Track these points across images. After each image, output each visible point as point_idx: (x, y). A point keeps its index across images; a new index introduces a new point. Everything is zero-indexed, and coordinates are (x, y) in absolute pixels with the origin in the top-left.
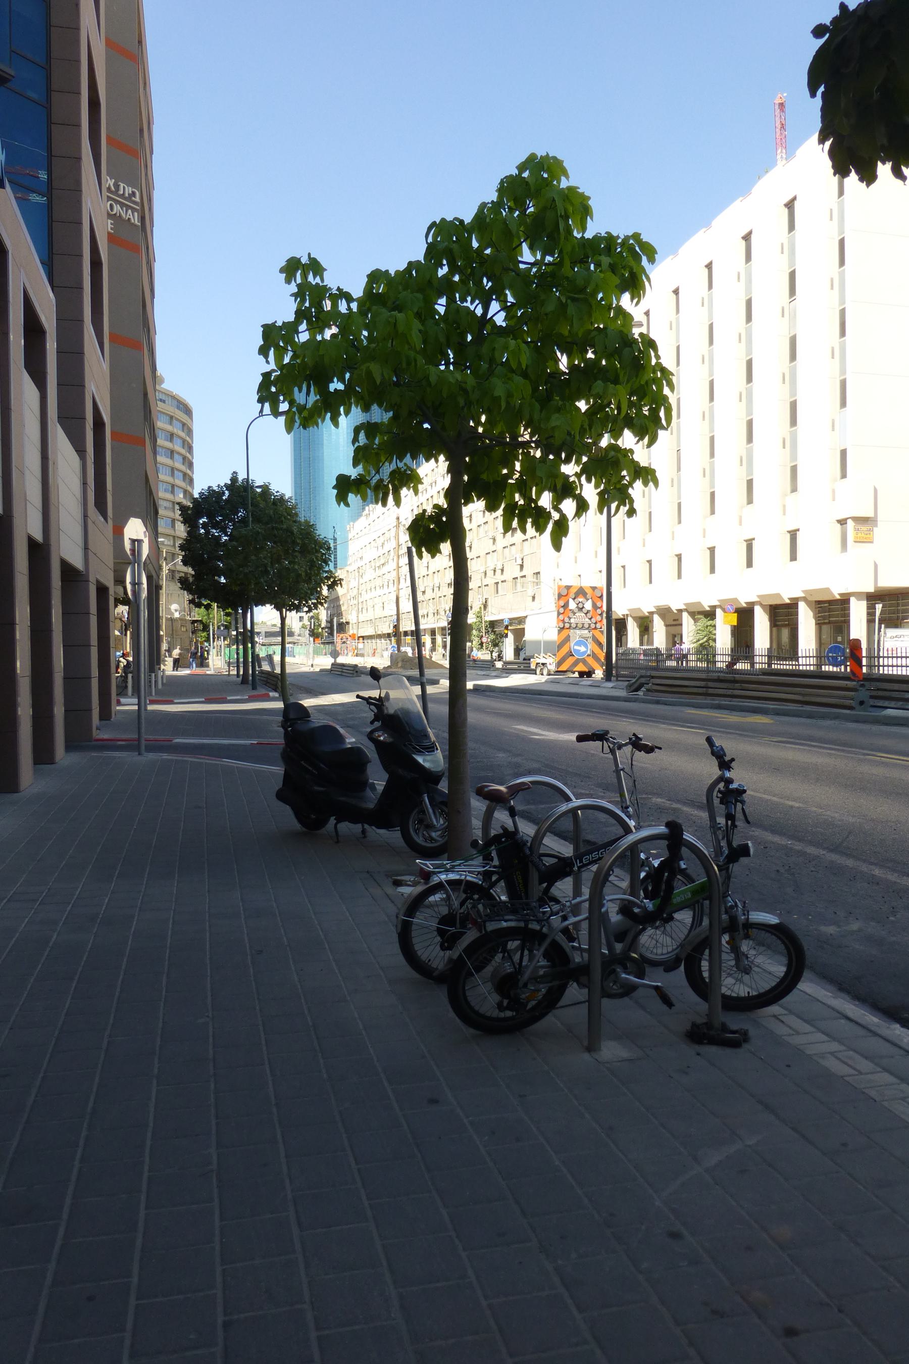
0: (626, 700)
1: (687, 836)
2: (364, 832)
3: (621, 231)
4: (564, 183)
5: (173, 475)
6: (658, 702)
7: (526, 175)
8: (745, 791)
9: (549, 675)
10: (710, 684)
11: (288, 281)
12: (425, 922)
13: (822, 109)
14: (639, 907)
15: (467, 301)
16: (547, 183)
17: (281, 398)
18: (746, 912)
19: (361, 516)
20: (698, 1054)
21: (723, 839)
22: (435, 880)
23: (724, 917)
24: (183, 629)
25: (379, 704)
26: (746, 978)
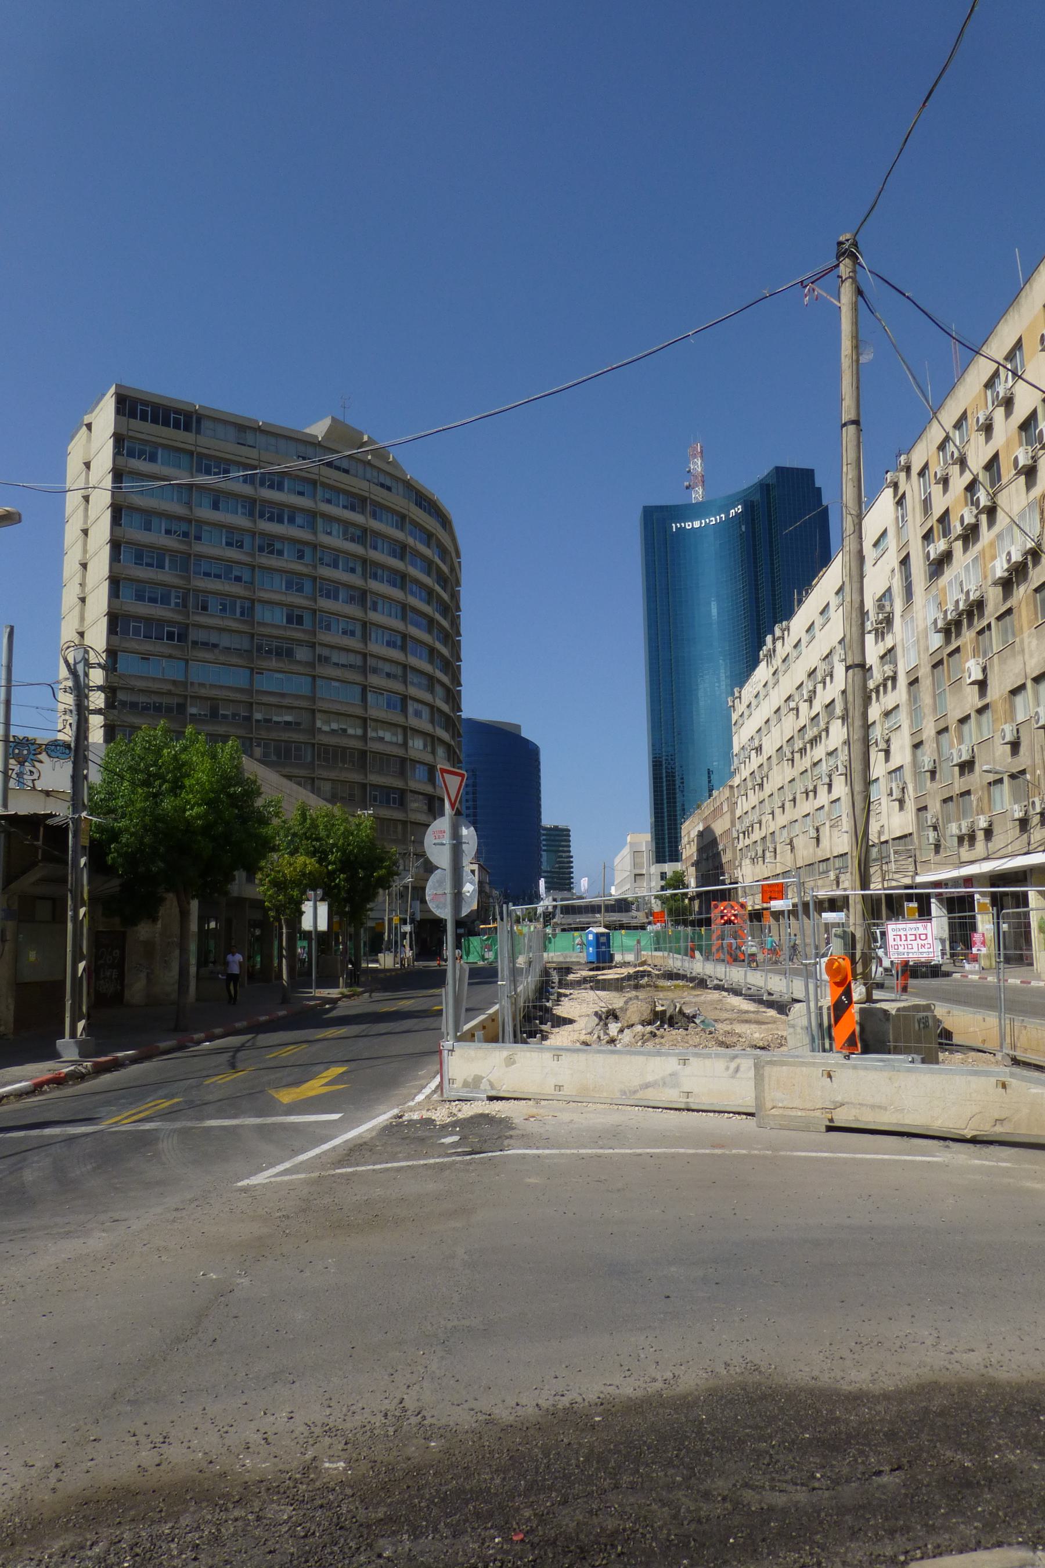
5: (404, 618)
19: (754, 663)
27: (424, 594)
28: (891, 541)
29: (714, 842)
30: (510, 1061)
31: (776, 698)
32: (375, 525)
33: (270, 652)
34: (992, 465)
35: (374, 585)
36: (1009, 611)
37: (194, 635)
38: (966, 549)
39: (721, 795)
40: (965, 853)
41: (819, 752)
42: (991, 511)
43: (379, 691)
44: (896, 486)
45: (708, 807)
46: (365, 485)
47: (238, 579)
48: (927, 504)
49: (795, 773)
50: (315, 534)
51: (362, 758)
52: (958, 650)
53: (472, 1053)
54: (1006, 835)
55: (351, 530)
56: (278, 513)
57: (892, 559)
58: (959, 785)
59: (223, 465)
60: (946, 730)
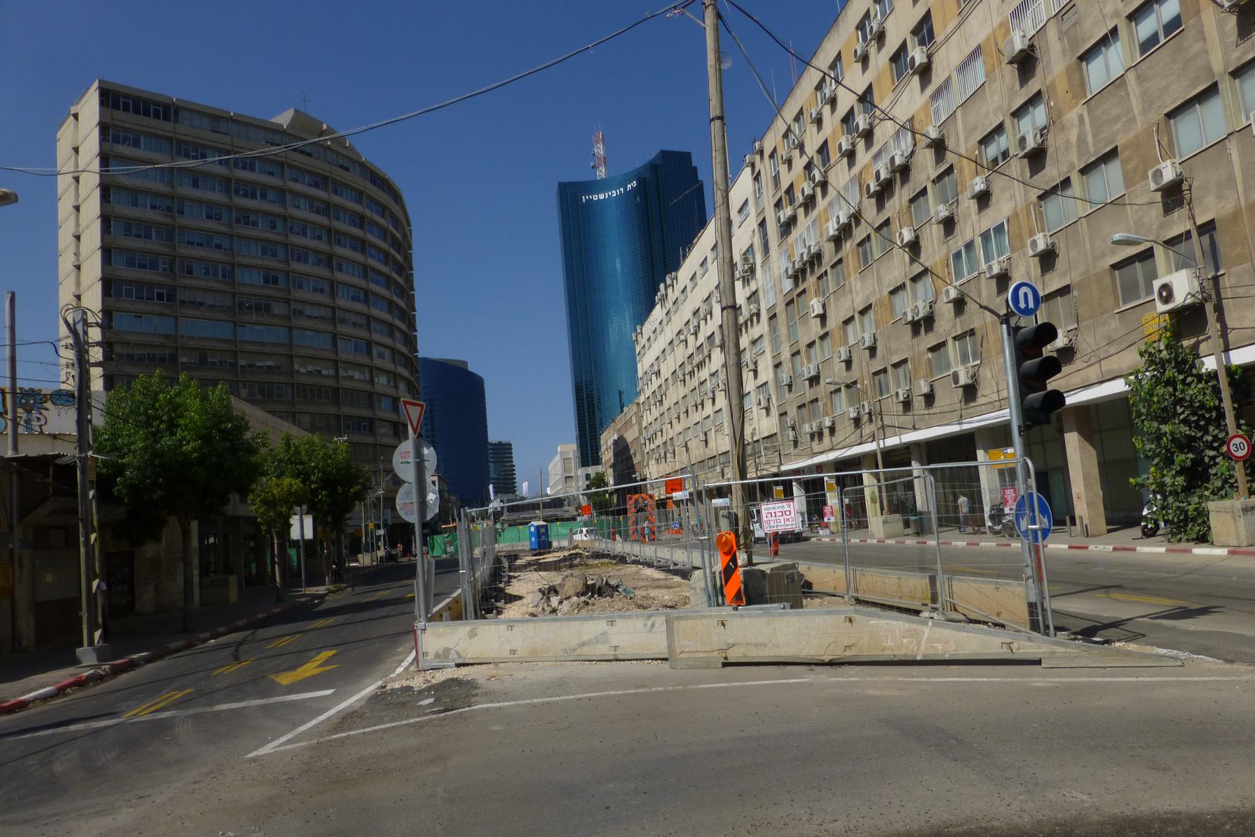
5: (365, 277)
19: (651, 306)
27: (381, 257)
28: (752, 209)
30: (472, 634)
31: (669, 333)
32: (336, 199)
33: (250, 308)
34: (823, 149)
35: (338, 250)
36: (840, 261)
37: (180, 295)
38: (806, 214)
39: (630, 410)
40: (816, 446)
41: (704, 374)
42: (824, 185)
43: (348, 337)
44: (753, 165)
45: (620, 420)
46: (327, 167)
47: (219, 247)
48: (776, 180)
49: (687, 390)
50: (285, 208)
51: (335, 394)
52: (804, 291)
53: (441, 630)
54: (845, 430)
55: (316, 204)
56: (251, 190)
57: (752, 222)
58: (809, 394)
59: (201, 151)
60: (798, 352)
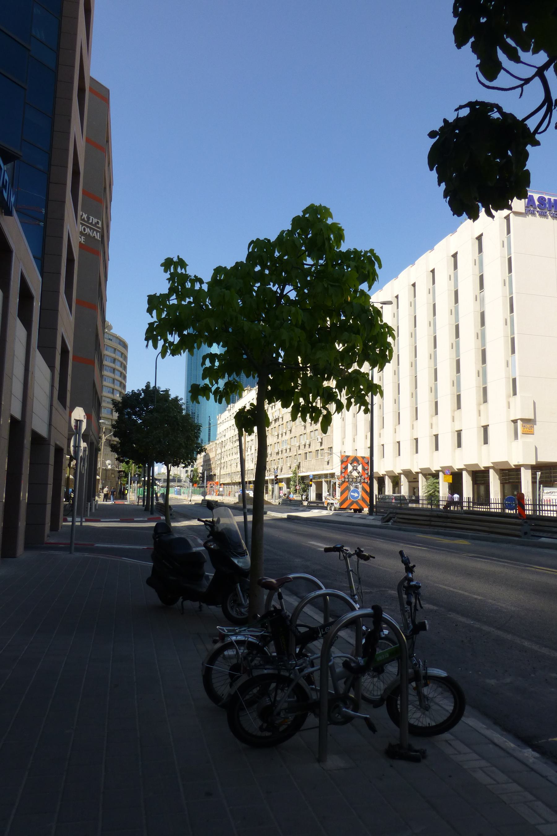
0: (380, 527)
1: (385, 615)
2: (200, 607)
3: (362, 247)
4: (330, 221)
5: (114, 383)
6: (400, 529)
7: (307, 216)
8: (420, 587)
9: (335, 510)
10: (433, 519)
11: (166, 271)
12: (221, 668)
13: (438, 178)
14: (354, 662)
15: (270, 285)
16: (320, 220)
17: (159, 338)
18: (425, 668)
19: (226, 410)
20: (391, 766)
21: (409, 618)
22: (228, 640)
23: (410, 671)
24: (113, 476)
25: (212, 525)
26: (427, 713)
29: (209, 460)
